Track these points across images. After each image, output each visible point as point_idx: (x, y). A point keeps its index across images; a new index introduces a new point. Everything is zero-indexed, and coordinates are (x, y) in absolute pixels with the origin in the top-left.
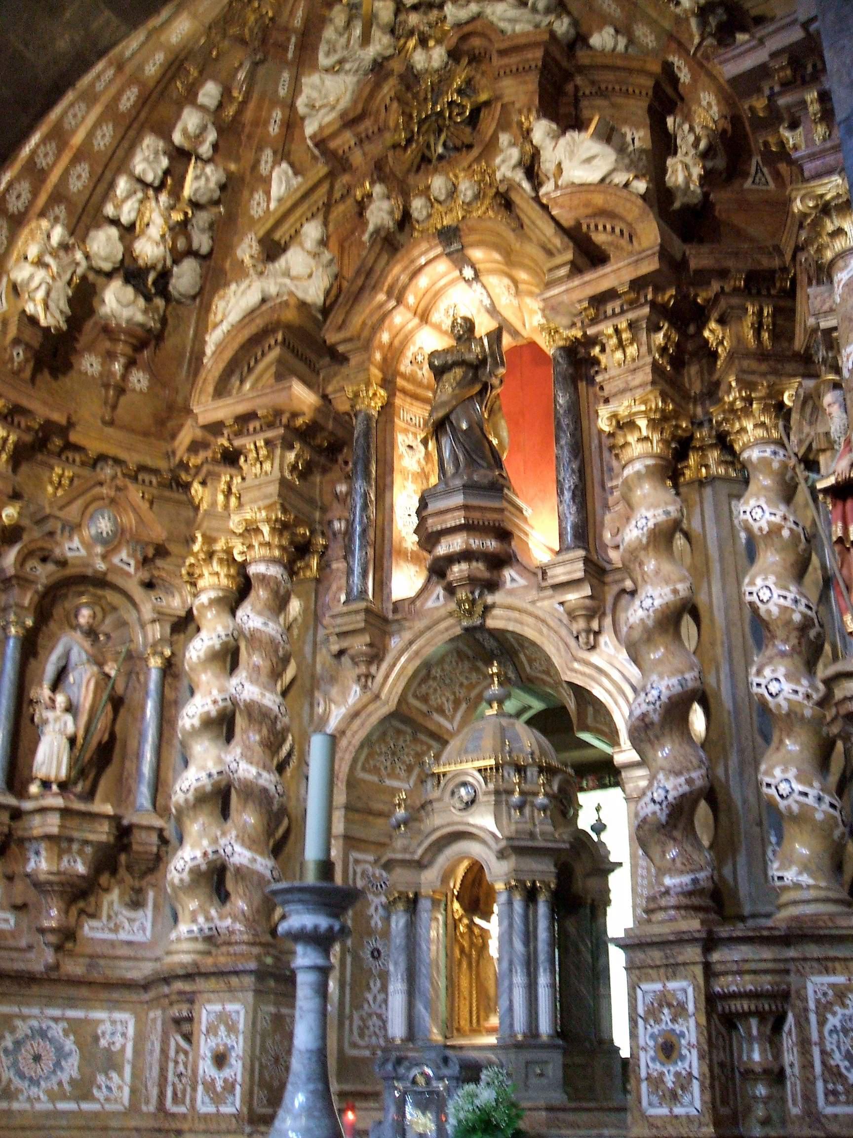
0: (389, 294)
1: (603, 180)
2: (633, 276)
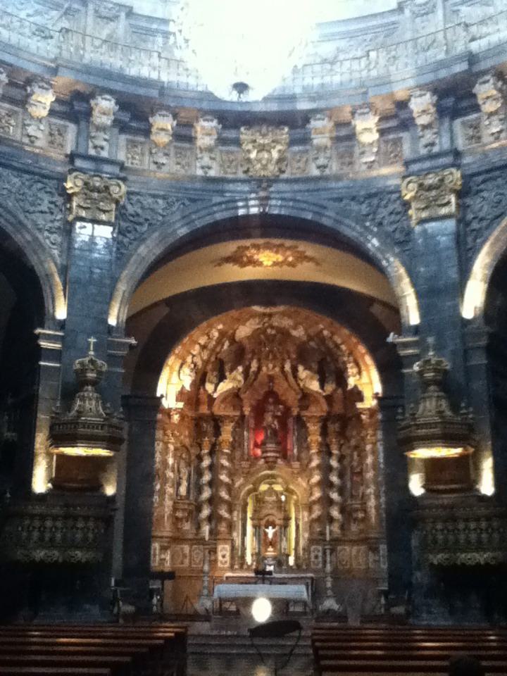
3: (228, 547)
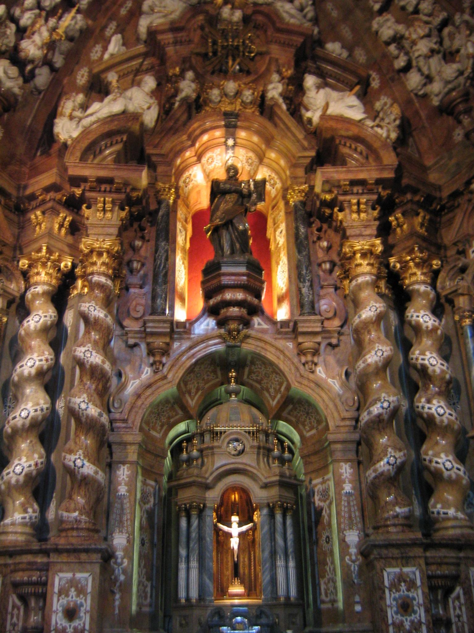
0: (189, 137)
1: (360, 121)
2: (378, 176)
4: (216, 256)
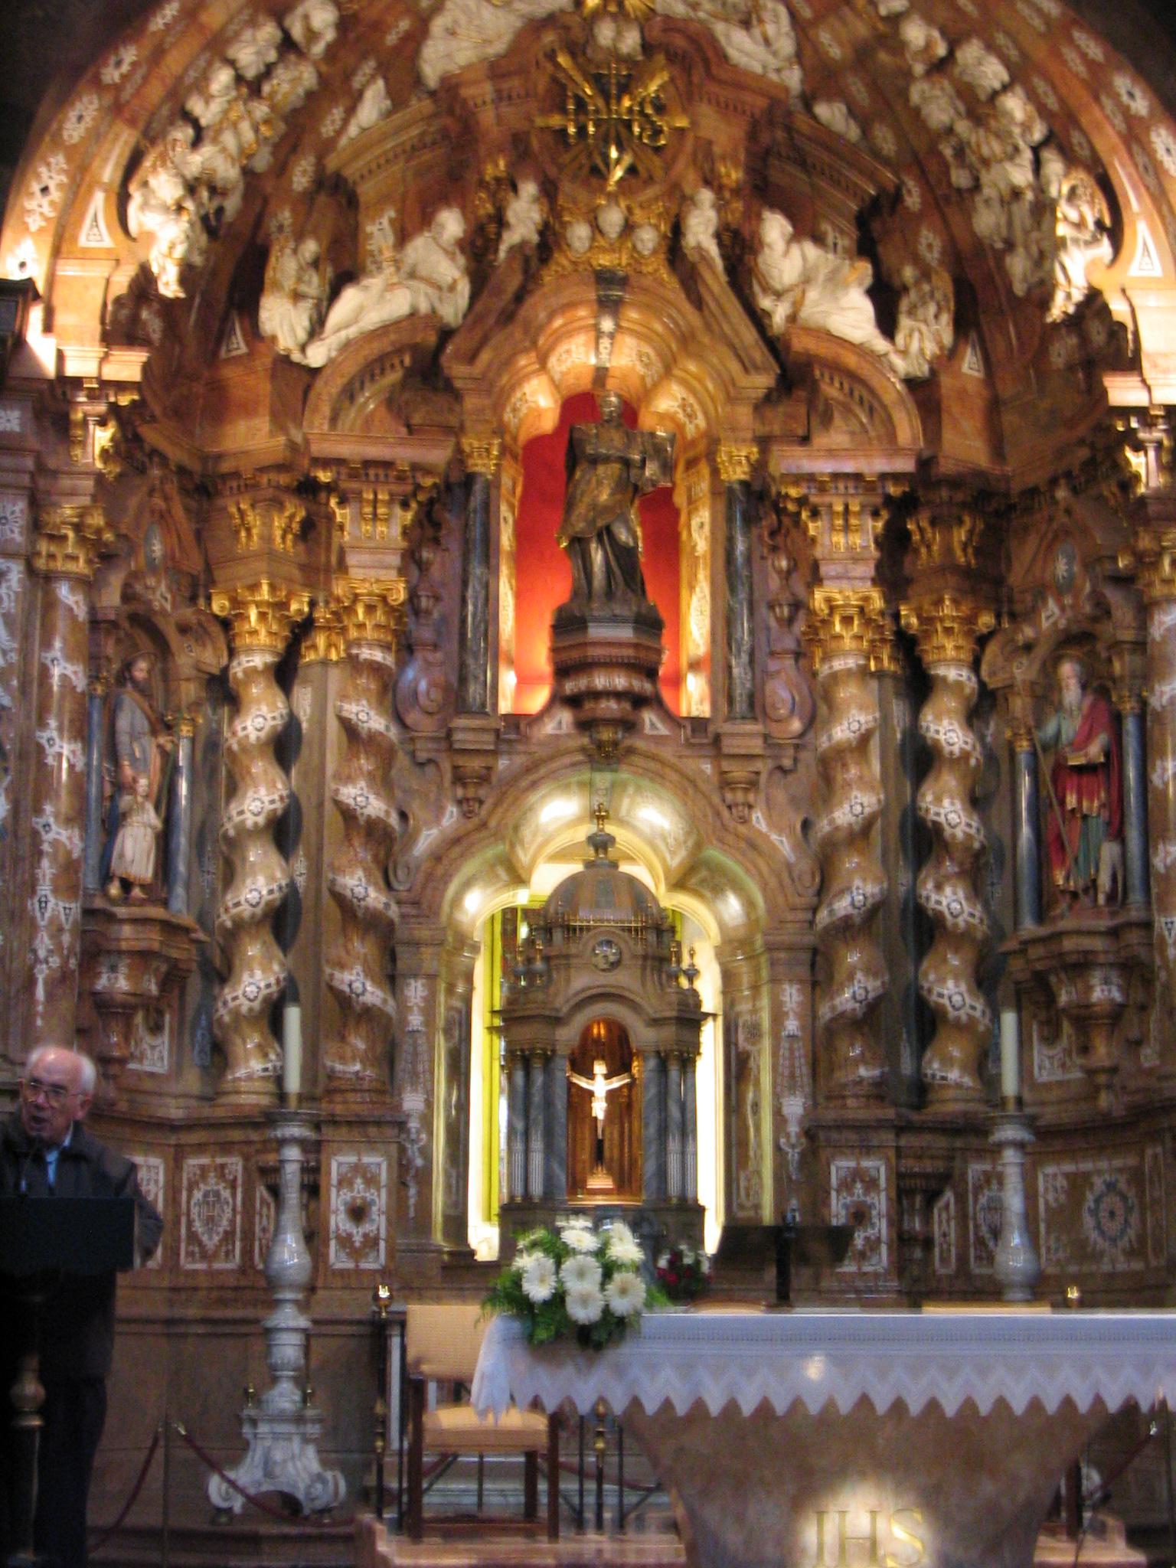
3: (378, 1162)
4: (575, 594)
